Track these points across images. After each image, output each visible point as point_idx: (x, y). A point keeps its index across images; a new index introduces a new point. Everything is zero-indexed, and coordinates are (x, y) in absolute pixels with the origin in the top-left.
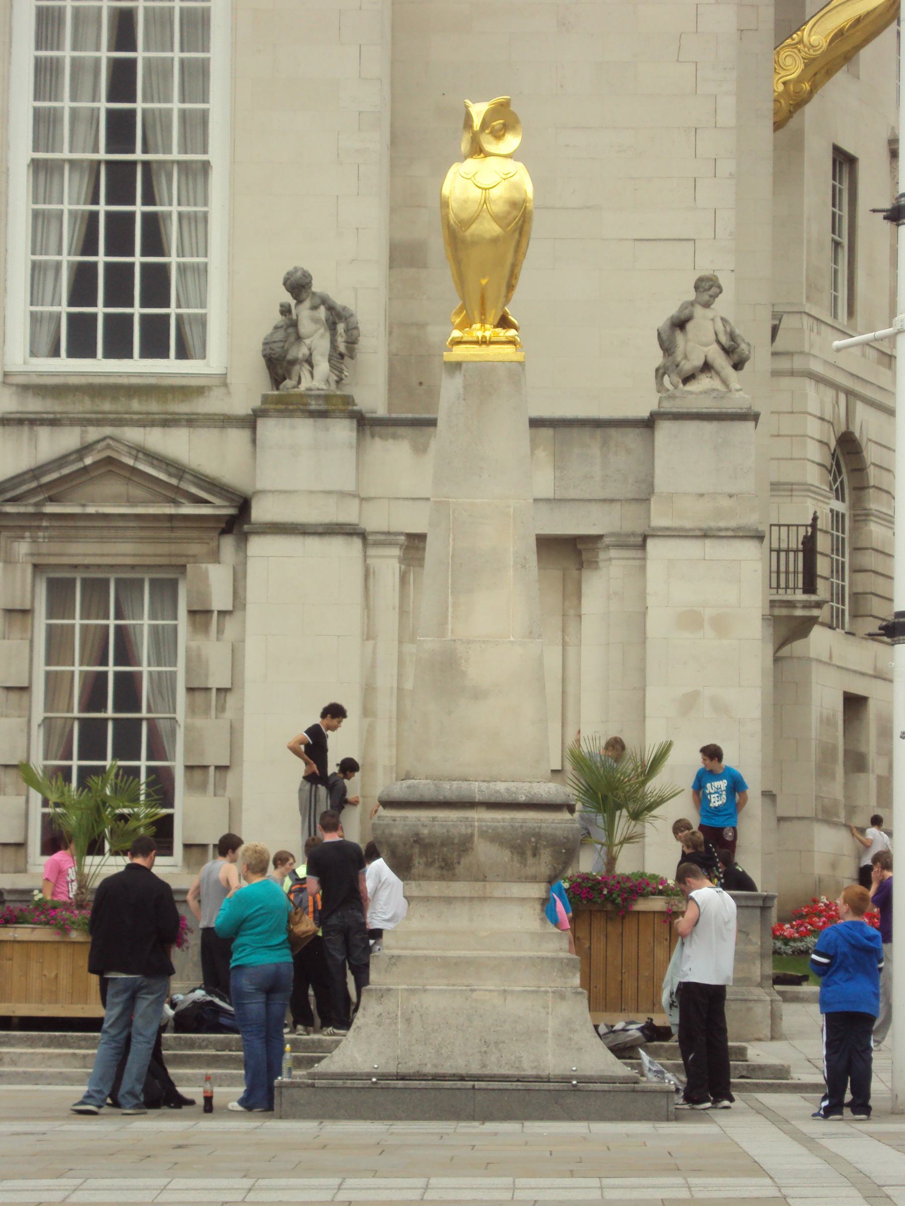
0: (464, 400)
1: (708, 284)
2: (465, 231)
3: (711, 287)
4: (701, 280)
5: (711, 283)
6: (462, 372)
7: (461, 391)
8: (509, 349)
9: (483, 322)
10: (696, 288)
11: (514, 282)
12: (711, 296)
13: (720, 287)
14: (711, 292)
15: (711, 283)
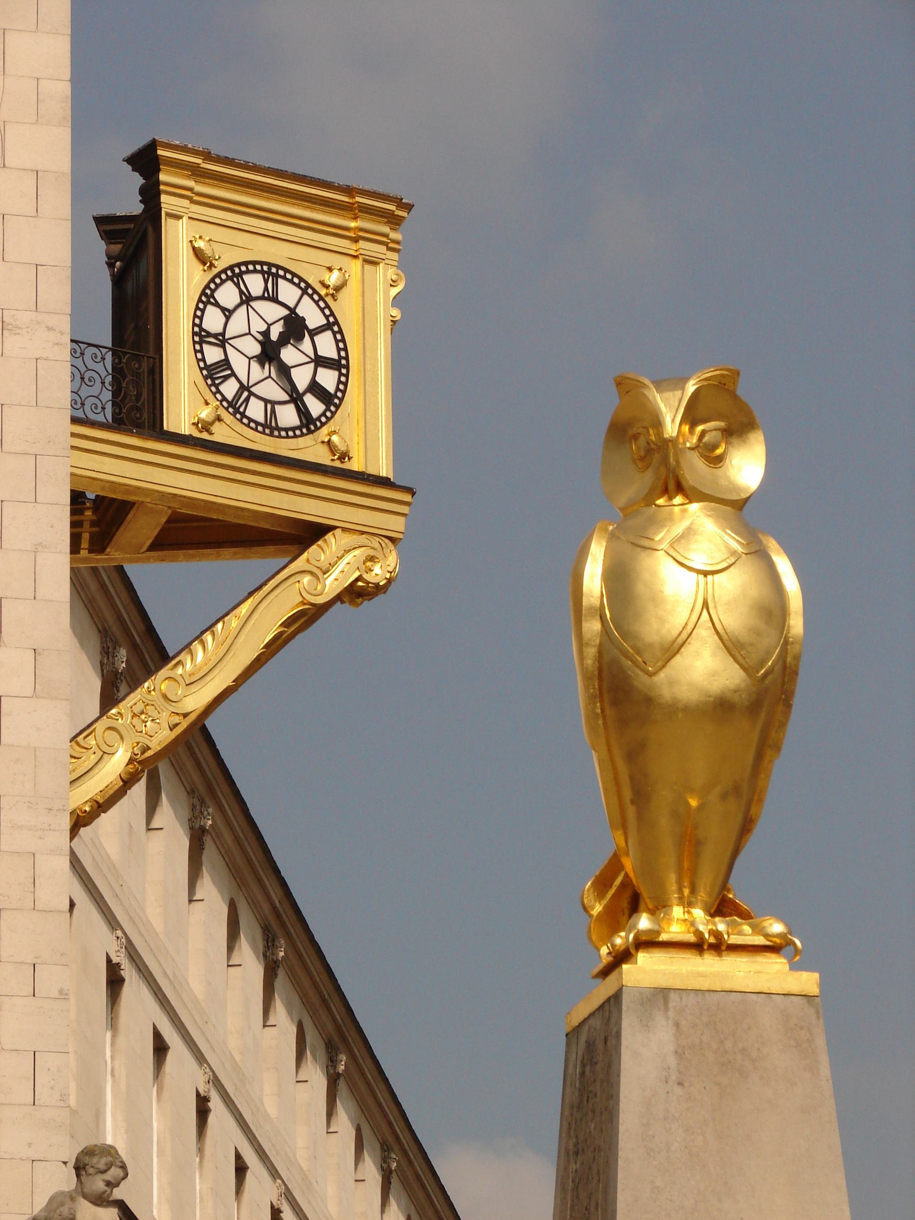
0: (680, 1084)
1: (104, 1160)
2: (655, 673)
3: (109, 1166)
4: (89, 1152)
5: (110, 1159)
6: (671, 1014)
7: (672, 1061)
8: (776, 964)
9: (688, 905)
10: (80, 1168)
11: (753, 810)
12: (108, 1184)
13: (123, 1167)
14: (108, 1176)
15: (110, 1159)
